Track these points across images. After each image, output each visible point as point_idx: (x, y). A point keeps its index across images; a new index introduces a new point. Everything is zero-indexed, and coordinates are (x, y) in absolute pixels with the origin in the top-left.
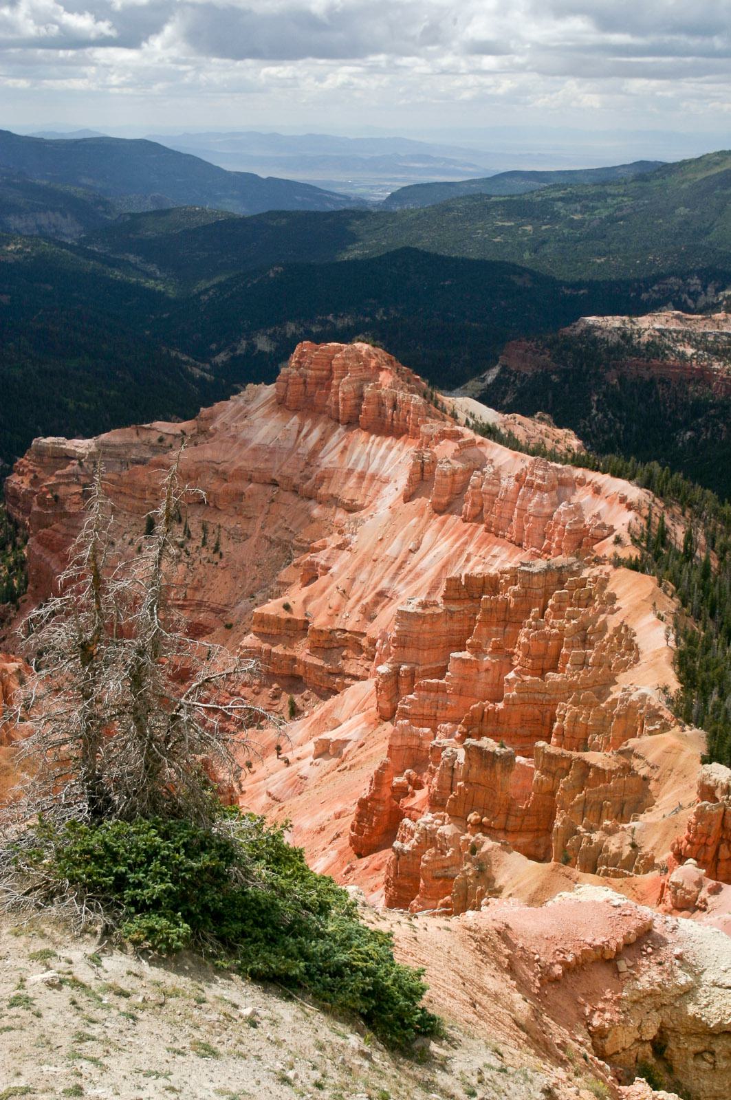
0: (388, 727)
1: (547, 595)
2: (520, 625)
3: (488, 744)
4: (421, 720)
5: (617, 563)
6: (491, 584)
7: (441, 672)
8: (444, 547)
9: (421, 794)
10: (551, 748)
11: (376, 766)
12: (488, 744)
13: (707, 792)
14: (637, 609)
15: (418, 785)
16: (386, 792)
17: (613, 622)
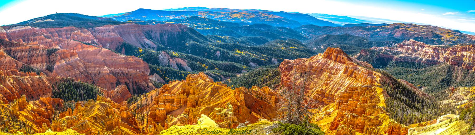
0: (338, 110)
1: (365, 91)
2: (361, 95)
3: (354, 114)
4: (343, 110)
5: (377, 86)
6: (356, 89)
7: (347, 102)
8: (349, 82)
9: (342, 122)
10: (365, 115)
11: (335, 116)
12: (354, 114)
13: (390, 123)
14: (380, 94)
15: (342, 120)
16: (336, 121)
17: (376, 96)
